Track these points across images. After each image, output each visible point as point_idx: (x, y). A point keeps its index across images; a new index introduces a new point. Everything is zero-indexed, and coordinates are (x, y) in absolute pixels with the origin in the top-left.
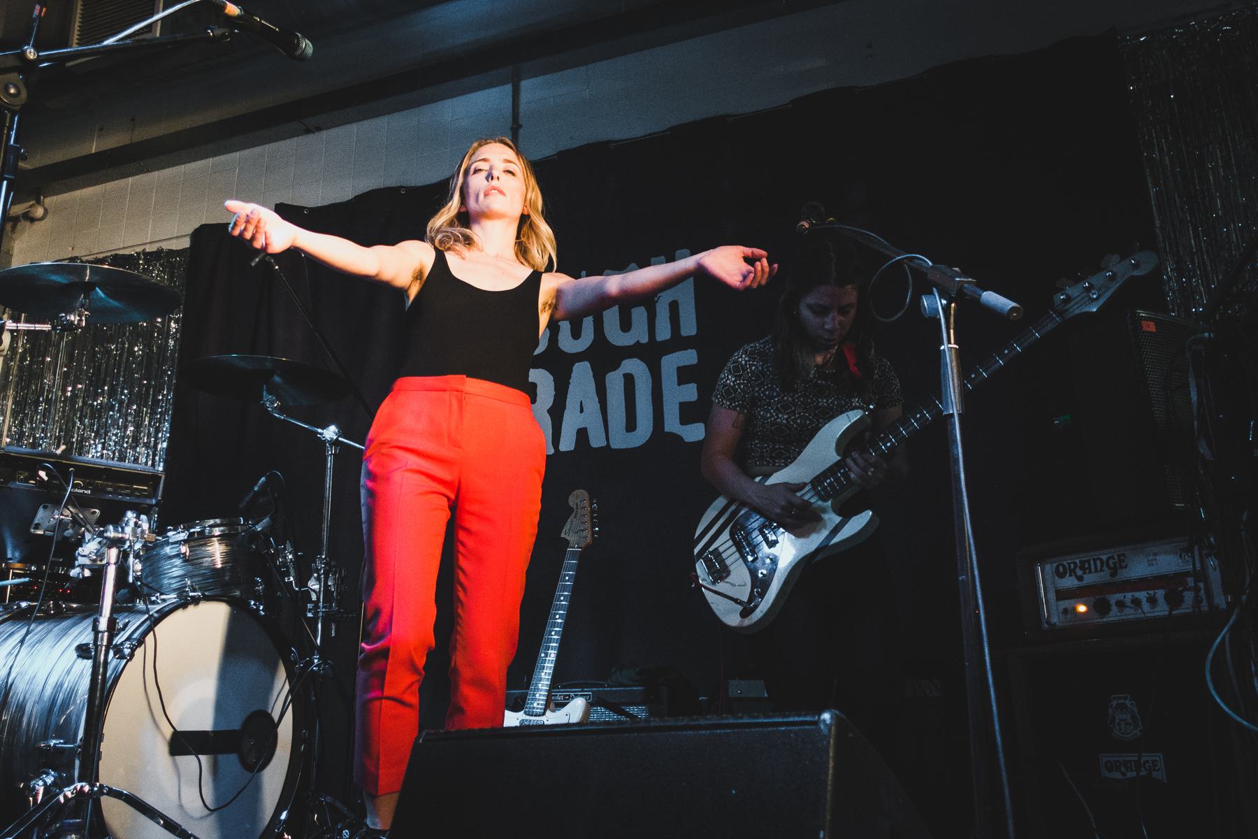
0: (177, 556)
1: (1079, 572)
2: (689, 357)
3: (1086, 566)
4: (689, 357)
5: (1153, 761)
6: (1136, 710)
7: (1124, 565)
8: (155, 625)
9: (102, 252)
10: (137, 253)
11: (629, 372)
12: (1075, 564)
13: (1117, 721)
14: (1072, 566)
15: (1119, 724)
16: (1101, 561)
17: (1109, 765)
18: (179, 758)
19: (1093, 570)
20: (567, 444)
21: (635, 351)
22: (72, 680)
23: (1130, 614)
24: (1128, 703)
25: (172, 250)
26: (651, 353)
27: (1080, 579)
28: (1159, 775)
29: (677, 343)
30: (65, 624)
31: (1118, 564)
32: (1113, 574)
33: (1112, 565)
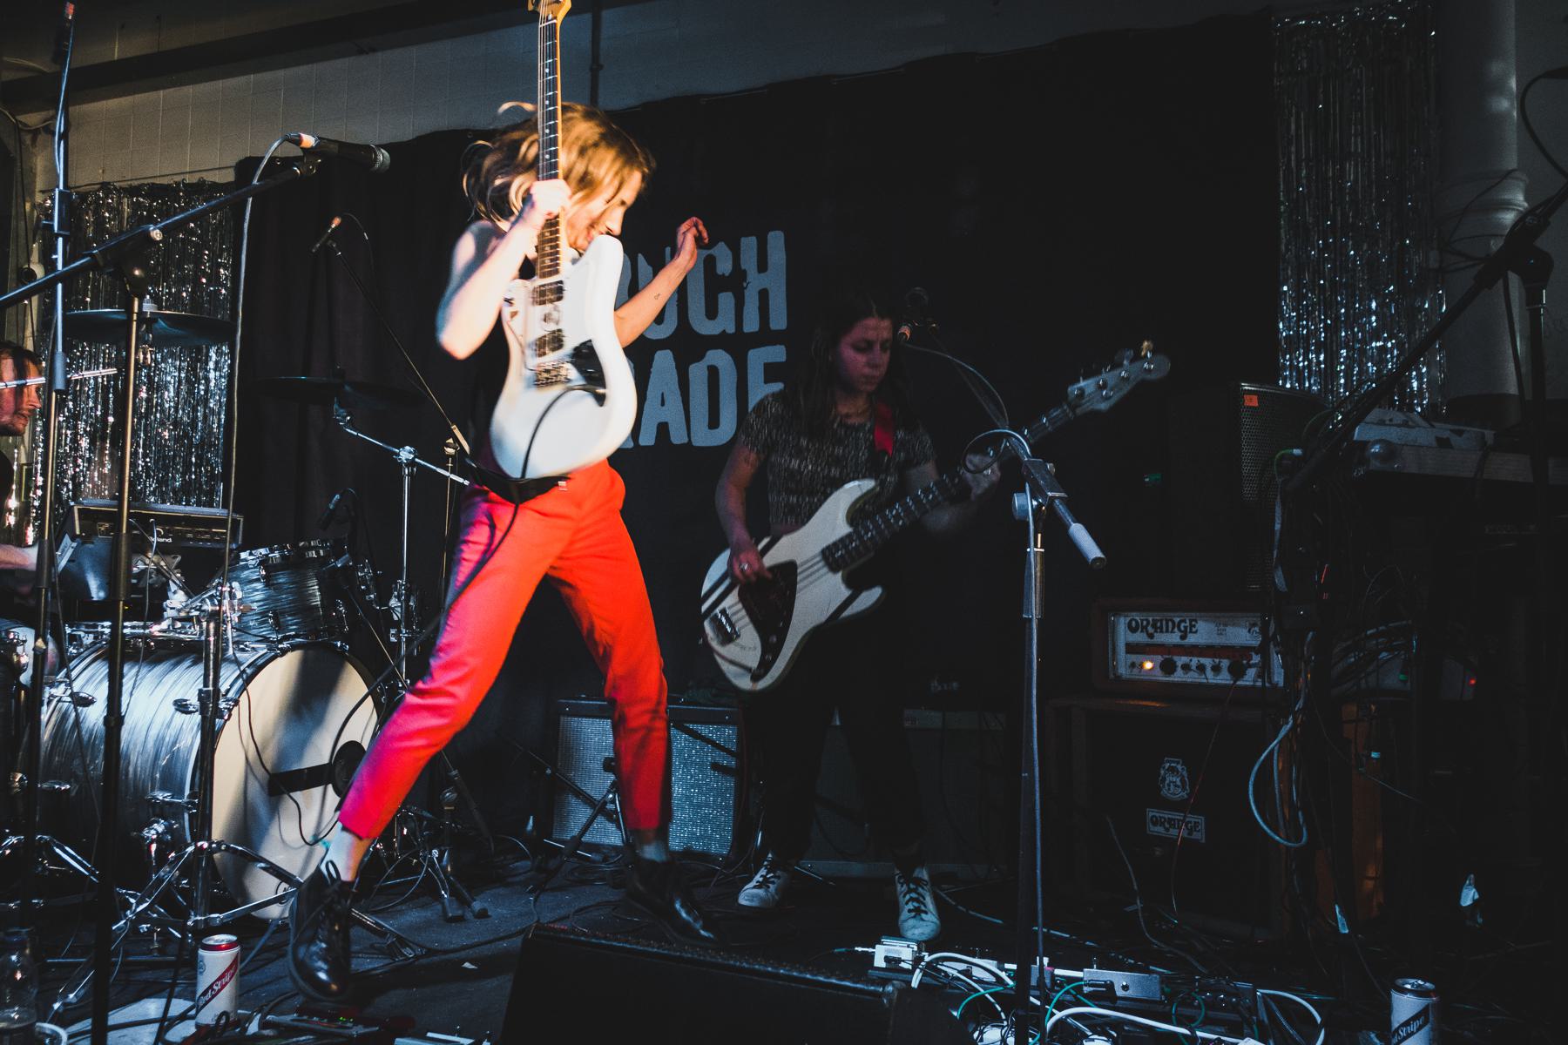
1: (1150, 630)
2: (777, 353)
3: (1159, 624)
4: (777, 353)
5: (1195, 822)
6: (1185, 773)
7: (1194, 630)
8: (248, 685)
9: (136, 179)
10: (176, 183)
12: (1148, 621)
13: (1167, 782)
14: (1145, 623)
15: (1169, 785)
16: (1173, 622)
17: (1154, 819)
19: (1164, 629)
20: (648, 439)
21: (720, 341)
22: (173, 734)
23: (1193, 677)
24: (1179, 767)
25: (215, 183)
26: (737, 345)
27: (1151, 636)
28: (1199, 836)
29: (766, 336)
30: (159, 669)
31: (1188, 630)
32: (1183, 638)
33: (1182, 629)
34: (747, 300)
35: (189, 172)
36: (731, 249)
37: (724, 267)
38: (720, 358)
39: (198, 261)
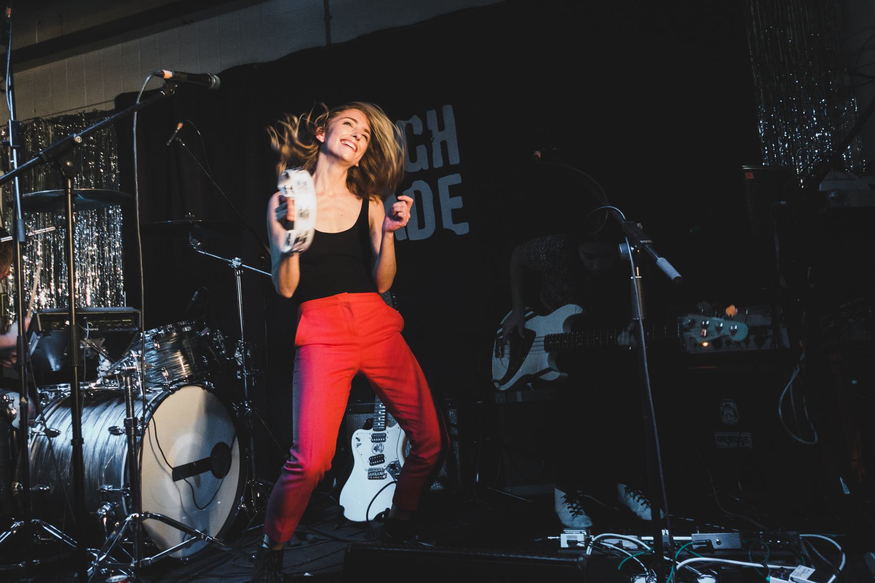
0: (153, 349)
2: (455, 179)
4: (455, 179)
5: (745, 437)
6: (736, 408)
9: (56, 114)
10: (79, 113)
11: (418, 189)
13: (725, 414)
15: (726, 416)
18: (177, 482)
21: (421, 175)
22: (110, 449)
24: (732, 404)
29: (448, 169)
30: (97, 410)
34: (434, 147)
35: (87, 106)
36: (421, 119)
37: (418, 130)
38: (421, 185)
39: (97, 160)
